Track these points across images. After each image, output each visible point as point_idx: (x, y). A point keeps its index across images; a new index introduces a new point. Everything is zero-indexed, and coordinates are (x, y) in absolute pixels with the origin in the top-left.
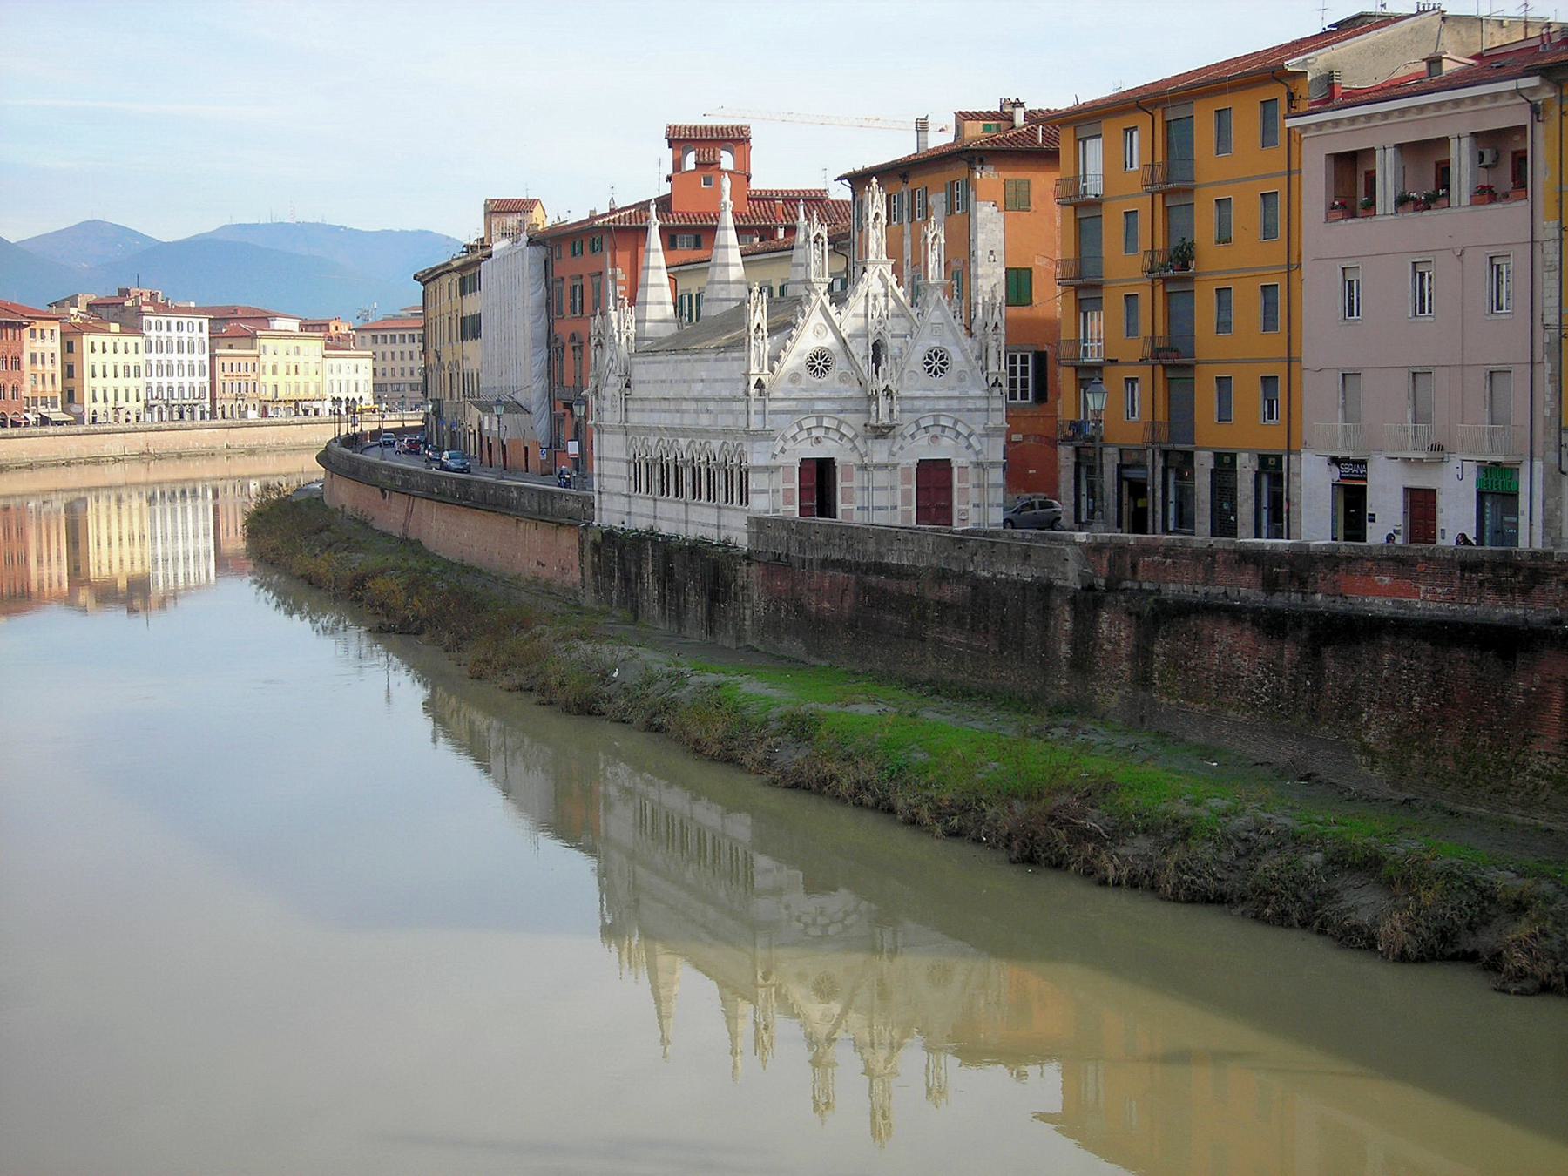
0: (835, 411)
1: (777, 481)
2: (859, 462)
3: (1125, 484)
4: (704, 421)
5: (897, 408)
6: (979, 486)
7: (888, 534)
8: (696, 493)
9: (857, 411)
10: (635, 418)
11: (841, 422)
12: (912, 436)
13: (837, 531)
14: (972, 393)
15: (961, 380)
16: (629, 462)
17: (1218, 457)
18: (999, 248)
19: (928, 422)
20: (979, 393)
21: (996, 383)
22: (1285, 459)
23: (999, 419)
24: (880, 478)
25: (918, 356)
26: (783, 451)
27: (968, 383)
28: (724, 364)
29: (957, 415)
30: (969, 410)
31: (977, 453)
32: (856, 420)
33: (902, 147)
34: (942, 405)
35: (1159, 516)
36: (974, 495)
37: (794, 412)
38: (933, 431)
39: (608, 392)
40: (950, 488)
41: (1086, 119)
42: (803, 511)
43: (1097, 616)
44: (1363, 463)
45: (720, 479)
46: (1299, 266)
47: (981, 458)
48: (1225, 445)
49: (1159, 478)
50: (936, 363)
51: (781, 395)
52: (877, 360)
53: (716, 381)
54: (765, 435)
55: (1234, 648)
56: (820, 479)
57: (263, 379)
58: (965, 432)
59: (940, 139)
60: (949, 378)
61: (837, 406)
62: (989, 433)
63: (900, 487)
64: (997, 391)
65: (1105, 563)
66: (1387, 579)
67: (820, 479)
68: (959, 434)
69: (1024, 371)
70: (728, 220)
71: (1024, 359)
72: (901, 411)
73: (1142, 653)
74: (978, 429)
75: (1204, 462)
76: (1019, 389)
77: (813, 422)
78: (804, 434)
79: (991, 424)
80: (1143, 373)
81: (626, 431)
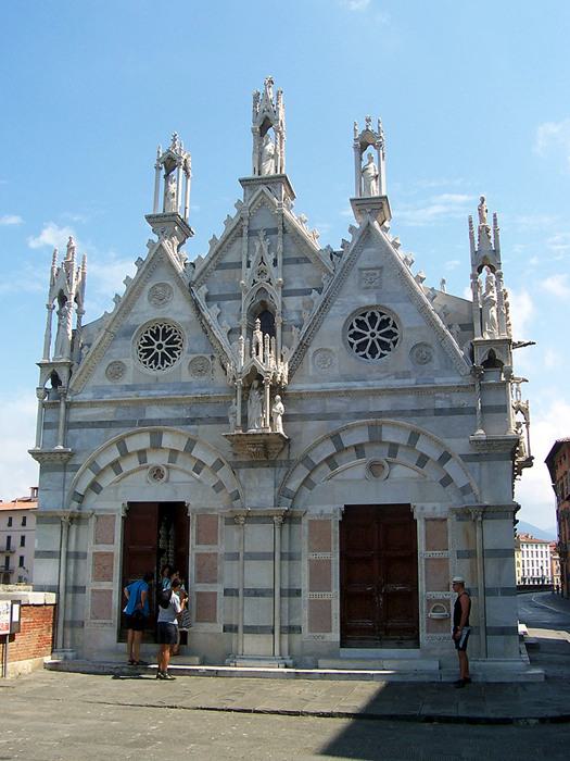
1: (86, 540)
6: (469, 554)
12: (331, 461)
14: (440, 381)
19: (360, 436)
20: (455, 380)
24: (261, 537)
25: (335, 322)
26: (95, 487)
27: (436, 364)
30: (439, 412)
34: (384, 404)
38: (374, 453)
40: (411, 558)
47: (469, 500)
50: (372, 334)
51: (87, 396)
61: (183, 413)
74: (459, 446)
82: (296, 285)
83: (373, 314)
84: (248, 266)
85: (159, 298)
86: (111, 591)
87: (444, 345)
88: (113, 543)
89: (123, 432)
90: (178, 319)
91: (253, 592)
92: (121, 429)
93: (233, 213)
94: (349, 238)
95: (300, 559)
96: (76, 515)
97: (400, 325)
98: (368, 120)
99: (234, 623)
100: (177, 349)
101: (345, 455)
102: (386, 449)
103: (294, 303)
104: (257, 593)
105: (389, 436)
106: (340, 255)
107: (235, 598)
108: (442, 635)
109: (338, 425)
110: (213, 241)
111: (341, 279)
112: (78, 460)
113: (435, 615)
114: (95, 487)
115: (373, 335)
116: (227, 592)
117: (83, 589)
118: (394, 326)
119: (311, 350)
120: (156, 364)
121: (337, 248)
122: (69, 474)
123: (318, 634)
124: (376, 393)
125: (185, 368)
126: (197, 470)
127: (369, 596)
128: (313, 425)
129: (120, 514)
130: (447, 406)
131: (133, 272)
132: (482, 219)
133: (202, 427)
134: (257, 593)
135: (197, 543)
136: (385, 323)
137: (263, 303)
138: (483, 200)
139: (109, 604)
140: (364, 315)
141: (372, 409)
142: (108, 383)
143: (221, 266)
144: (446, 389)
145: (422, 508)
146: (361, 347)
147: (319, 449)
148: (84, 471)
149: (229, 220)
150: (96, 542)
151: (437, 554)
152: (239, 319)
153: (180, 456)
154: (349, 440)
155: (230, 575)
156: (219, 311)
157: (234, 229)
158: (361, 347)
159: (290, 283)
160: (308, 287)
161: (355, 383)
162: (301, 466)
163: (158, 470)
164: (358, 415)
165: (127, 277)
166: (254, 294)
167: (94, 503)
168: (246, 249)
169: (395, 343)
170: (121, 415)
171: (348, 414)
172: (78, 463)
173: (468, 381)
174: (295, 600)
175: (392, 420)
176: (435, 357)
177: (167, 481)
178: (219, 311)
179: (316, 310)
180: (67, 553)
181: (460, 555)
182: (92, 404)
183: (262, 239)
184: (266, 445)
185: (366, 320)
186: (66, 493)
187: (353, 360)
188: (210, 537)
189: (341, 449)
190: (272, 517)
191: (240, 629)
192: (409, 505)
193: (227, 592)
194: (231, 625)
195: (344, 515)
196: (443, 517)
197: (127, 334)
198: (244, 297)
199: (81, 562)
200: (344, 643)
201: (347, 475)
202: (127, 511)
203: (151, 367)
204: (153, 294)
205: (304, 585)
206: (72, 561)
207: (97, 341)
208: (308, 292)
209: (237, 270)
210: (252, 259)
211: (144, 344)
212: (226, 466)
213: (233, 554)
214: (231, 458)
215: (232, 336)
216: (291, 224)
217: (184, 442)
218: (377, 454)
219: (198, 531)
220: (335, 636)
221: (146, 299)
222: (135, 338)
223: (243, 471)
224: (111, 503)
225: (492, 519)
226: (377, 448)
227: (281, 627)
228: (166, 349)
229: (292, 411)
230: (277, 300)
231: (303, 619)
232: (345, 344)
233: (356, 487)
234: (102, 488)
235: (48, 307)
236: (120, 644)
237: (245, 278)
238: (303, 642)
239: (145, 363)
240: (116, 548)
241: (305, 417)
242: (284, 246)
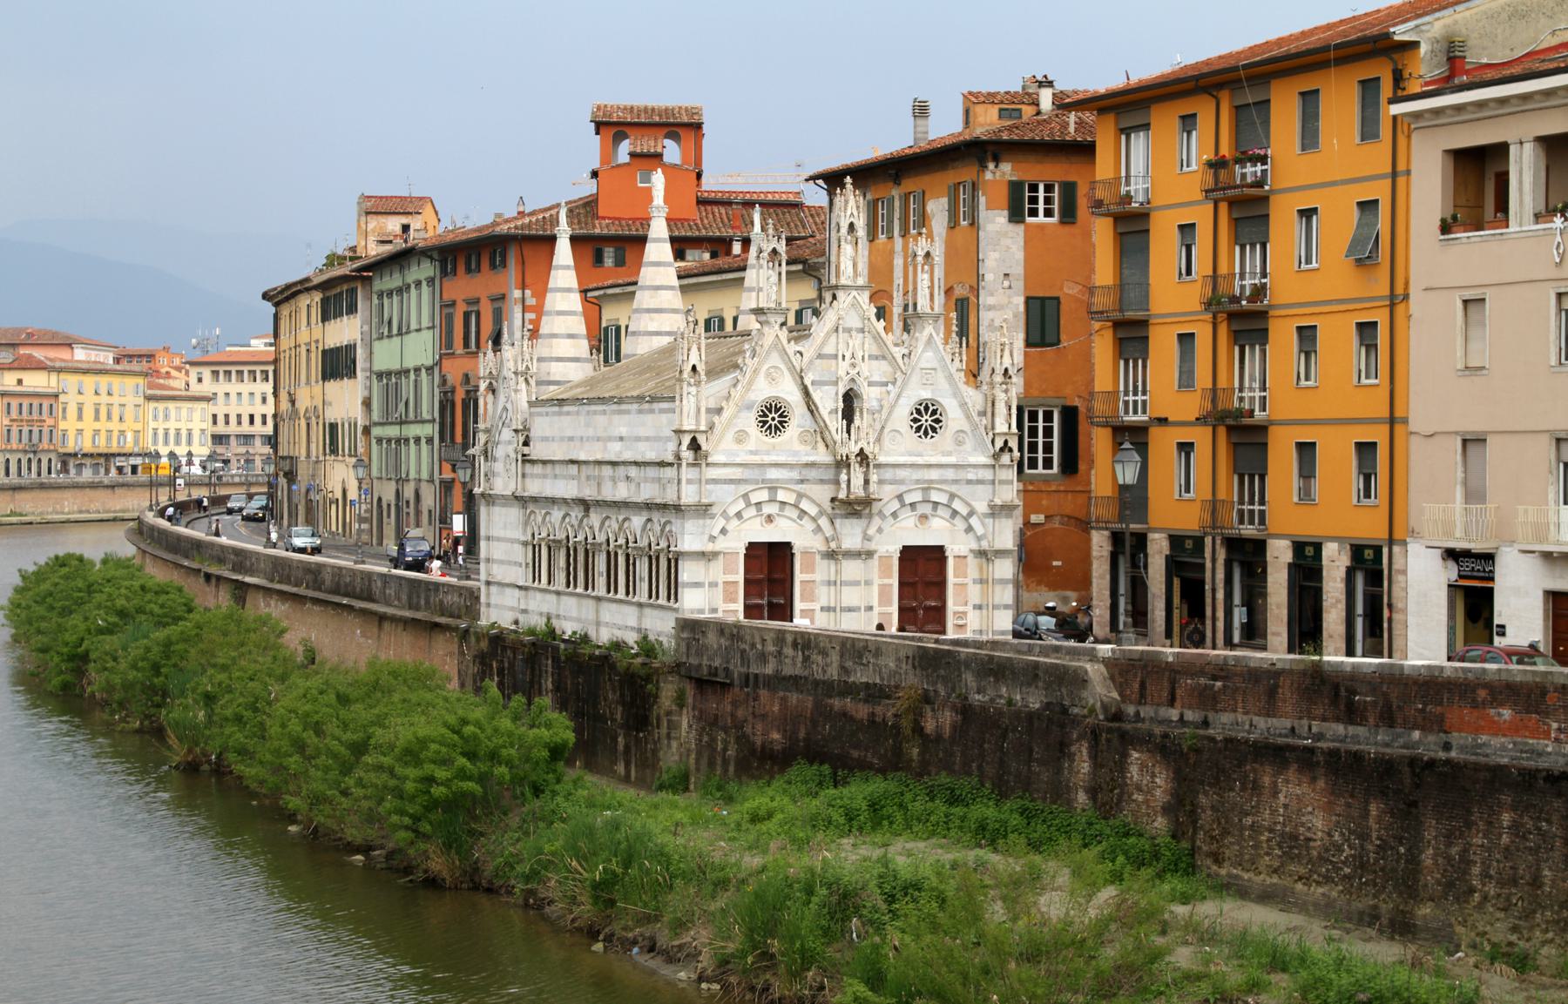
0: (790, 481)
2: (823, 548)
3: (1176, 582)
4: (622, 492)
5: (874, 478)
6: (981, 581)
7: (854, 649)
8: (611, 585)
9: (822, 481)
10: (534, 488)
11: (800, 496)
12: (894, 515)
13: (789, 639)
14: (973, 460)
15: (959, 443)
16: (525, 544)
17: (1299, 547)
18: (1018, 270)
21: (1006, 447)
22: (1385, 551)
23: (1010, 492)
24: (851, 569)
26: (723, 531)
27: (968, 446)
28: (650, 417)
29: (953, 488)
30: (969, 482)
31: (979, 539)
32: (823, 493)
33: (896, 139)
34: (934, 474)
35: (1220, 625)
39: (500, 452)
41: (1130, 106)
42: (750, 611)
43: (1125, 756)
44: (1489, 558)
45: (642, 567)
46: (1406, 297)
47: (985, 545)
48: (1308, 529)
49: (1220, 575)
50: (926, 420)
52: (848, 415)
53: (638, 439)
54: (703, 510)
55: (1302, 804)
56: (770, 568)
57: (62, 425)
58: (964, 511)
59: (945, 126)
60: (945, 437)
61: (795, 475)
62: (998, 511)
63: (877, 581)
64: (1006, 458)
65: (1136, 686)
66: (1507, 713)
67: (770, 568)
68: (955, 513)
69: (1048, 432)
70: (659, 229)
71: (1048, 417)
72: (881, 482)
73: (1181, 807)
74: (982, 507)
75: (1280, 555)
76: (1040, 455)
77: (763, 495)
78: (752, 511)
79: (998, 502)
80: (1201, 437)
81: (521, 500)
82: (876, 378)
85: (771, 379)
90: (789, 398)
104: (850, 610)
105: (935, 496)
109: (903, 488)
112: (714, 510)
119: (886, 431)
124: (930, 466)
125: (795, 439)
127: (914, 609)
134: (850, 610)
136: (934, 412)
142: (735, 447)
143: (820, 356)
144: (975, 466)
146: (918, 429)
167: (721, 544)
173: (990, 461)
181: (975, 582)
182: (725, 465)
188: (809, 567)
197: (749, 407)
201: (904, 524)
204: (768, 375)
205: (875, 603)
208: (886, 384)
209: (833, 362)
210: (848, 356)
214: (829, 511)
217: (794, 496)
240: (740, 577)
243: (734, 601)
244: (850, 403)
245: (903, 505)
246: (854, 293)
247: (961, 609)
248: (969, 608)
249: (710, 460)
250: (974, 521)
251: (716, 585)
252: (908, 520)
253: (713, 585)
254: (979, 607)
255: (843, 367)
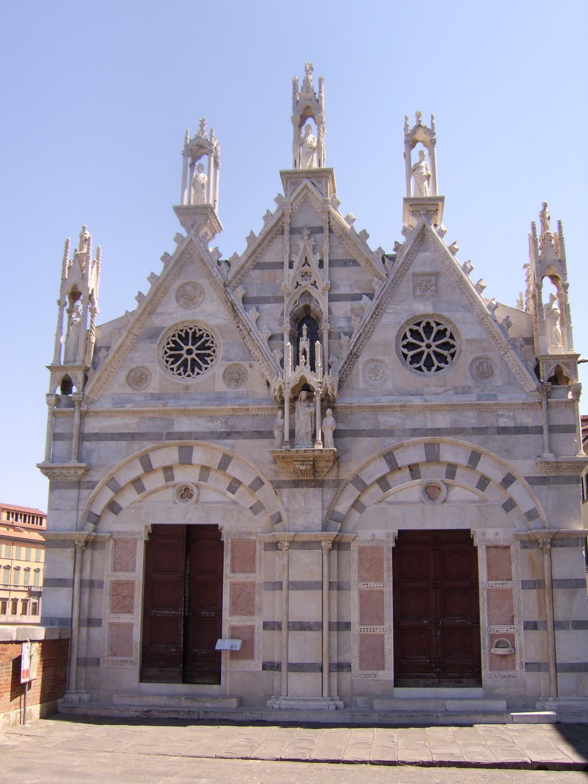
1: (103, 567)
6: (537, 584)
14: (502, 398)
19: (416, 455)
20: (519, 398)
24: (308, 565)
26: (113, 507)
27: (498, 380)
30: (503, 430)
34: (442, 421)
36: (526, 604)
37: (132, 437)
50: (428, 346)
74: (524, 467)
79: (548, 456)
82: (344, 290)
83: (428, 323)
84: (291, 267)
85: (187, 298)
86: (132, 625)
87: (506, 359)
88: (134, 570)
89: (149, 445)
91: (299, 626)
92: (145, 443)
93: (273, 208)
94: (402, 240)
95: (350, 589)
96: (91, 538)
97: (459, 336)
98: (418, 115)
99: (276, 661)
100: (209, 355)
101: (398, 475)
102: (444, 469)
103: (342, 309)
104: (303, 627)
105: (447, 455)
106: (392, 258)
107: (277, 632)
108: (506, 673)
110: (251, 238)
111: (395, 283)
112: (94, 476)
113: (500, 651)
114: (113, 507)
115: (428, 346)
116: (266, 625)
117: (98, 623)
118: (452, 337)
120: (185, 371)
121: (389, 251)
122: (85, 493)
123: (370, 672)
126: (232, 489)
128: (365, 443)
129: (144, 537)
130: (509, 423)
131: (159, 268)
132: (545, 226)
133: (240, 442)
134: (303, 627)
135: (233, 571)
137: (307, 308)
138: (545, 205)
139: (129, 639)
140: (418, 324)
141: (429, 426)
142: (129, 390)
143: (259, 266)
144: (509, 406)
145: (484, 534)
146: (416, 358)
147: (371, 468)
148: (101, 489)
149: (268, 216)
150: (115, 569)
151: (498, 585)
152: (281, 324)
153: (213, 474)
154: (404, 458)
155: (271, 606)
156: (258, 314)
157: (275, 225)
158: (416, 358)
159: (339, 287)
160: (357, 292)
161: (411, 398)
162: (351, 487)
163: (187, 489)
164: (415, 432)
165: (152, 274)
166: (297, 297)
168: (288, 248)
169: (453, 355)
170: (145, 427)
171: (404, 431)
172: (94, 479)
173: (536, 398)
174: (345, 633)
175: (451, 438)
176: (497, 372)
177: (197, 501)
178: (258, 314)
179: (367, 316)
180: (82, 582)
181: (525, 585)
183: (306, 238)
184: (315, 461)
185: (421, 330)
186: (81, 513)
187: (407, 372)
188: (247, 562)
189: (394, 467)
190: (319, 542)
191: (284, 667)
192: (469, 531)
193: (266, 625)
194: (273, 663)
195: (396, 541)
196: (506, 544)
197: (153, 335)
198: (287, 300)
199: (97, 591)
200: (397, 683)
202: (149, 534)
203: (180, 374)
205: (353, 615)
206: (87, 590)
207: (118, 344)
209: (279, 271)
211: (171, 349)
212: (268, 487)
213: (274, 583)
215: (273, 342)
216: (338, 222)
218: (434, 474)
219: (233, 558)
220: (388, 674)
221: (174, 300)
222: (160, 342)
223: (285, 491)
224: (133, 525)
225: (562, 546)
226: (434, 468)
227: (330, 665)
228: (197, 355)
229: (342, 427)
230: (323, 305)
231: (353, 656)
232: (398, 355)
233: (410, 509)
234: (122, 509)
235: (59, 303)
236: (147, 686)
237: (288, 277)
238: (352, 681)
239: (172, 369)
240: (137, 576)
241: (357, 433)
242: (330, 247)
243: (129, 610)
244: (306, 321)
245: (394, 467)
246: (306, 182)
247: (503, 629)
248: (519, 627)
249: (84, 408)
250: (516, 491)
251: (101, 585)
252: (407, 489)
253: (92, 584)
254: (531, 626)
255: (288, 277)
